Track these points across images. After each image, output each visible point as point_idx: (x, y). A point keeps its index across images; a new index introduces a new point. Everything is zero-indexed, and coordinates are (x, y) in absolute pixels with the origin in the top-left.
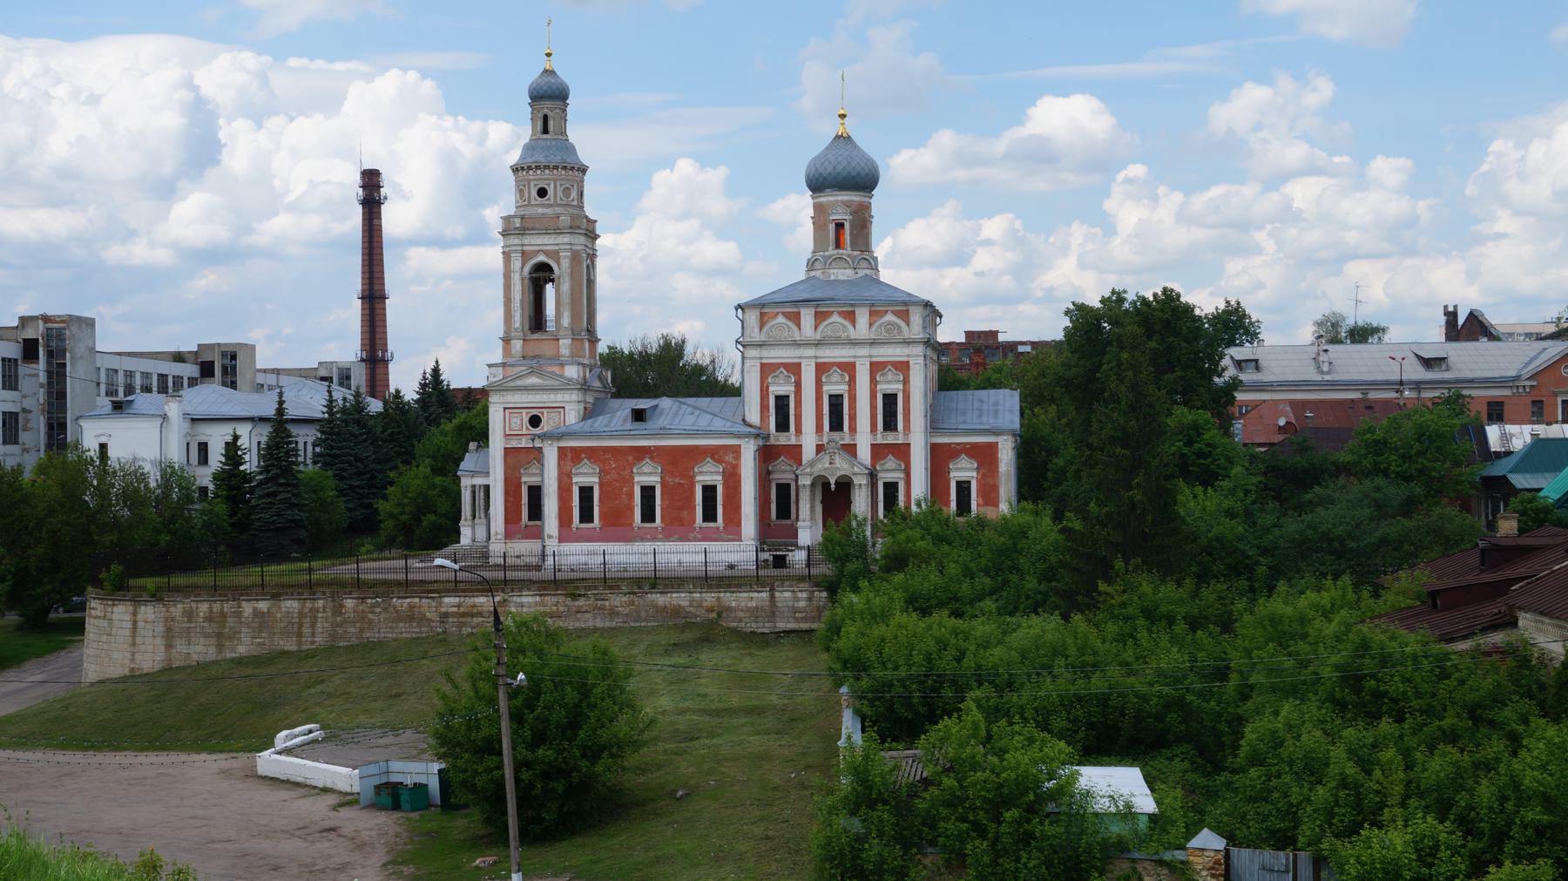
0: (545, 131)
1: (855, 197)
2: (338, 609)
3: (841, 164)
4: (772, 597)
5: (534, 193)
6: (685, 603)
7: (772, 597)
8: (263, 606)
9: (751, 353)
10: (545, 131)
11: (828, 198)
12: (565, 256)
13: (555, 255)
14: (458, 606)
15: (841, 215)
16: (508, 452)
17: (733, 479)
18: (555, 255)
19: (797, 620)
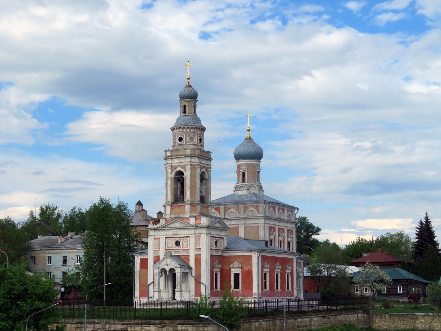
0: (185, 112)
1: (254, 162)
2: (275, 325)
3: (250, 149)
4: (358, 316)
5: (199, 140)
6: (344, 319)
7: (358, 316)
8: (257, 324)
9: (267, 221)
10: (185, 112)
11: (242, 162)
12: (188, 168)
13: (184, 167)
14: (301, 322)
15: (243, 169)
16: (212, 256)
17: (292, 270)
18: (184, 167)
19: (363, 325)
